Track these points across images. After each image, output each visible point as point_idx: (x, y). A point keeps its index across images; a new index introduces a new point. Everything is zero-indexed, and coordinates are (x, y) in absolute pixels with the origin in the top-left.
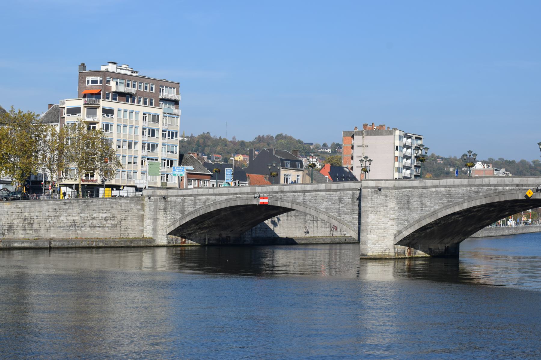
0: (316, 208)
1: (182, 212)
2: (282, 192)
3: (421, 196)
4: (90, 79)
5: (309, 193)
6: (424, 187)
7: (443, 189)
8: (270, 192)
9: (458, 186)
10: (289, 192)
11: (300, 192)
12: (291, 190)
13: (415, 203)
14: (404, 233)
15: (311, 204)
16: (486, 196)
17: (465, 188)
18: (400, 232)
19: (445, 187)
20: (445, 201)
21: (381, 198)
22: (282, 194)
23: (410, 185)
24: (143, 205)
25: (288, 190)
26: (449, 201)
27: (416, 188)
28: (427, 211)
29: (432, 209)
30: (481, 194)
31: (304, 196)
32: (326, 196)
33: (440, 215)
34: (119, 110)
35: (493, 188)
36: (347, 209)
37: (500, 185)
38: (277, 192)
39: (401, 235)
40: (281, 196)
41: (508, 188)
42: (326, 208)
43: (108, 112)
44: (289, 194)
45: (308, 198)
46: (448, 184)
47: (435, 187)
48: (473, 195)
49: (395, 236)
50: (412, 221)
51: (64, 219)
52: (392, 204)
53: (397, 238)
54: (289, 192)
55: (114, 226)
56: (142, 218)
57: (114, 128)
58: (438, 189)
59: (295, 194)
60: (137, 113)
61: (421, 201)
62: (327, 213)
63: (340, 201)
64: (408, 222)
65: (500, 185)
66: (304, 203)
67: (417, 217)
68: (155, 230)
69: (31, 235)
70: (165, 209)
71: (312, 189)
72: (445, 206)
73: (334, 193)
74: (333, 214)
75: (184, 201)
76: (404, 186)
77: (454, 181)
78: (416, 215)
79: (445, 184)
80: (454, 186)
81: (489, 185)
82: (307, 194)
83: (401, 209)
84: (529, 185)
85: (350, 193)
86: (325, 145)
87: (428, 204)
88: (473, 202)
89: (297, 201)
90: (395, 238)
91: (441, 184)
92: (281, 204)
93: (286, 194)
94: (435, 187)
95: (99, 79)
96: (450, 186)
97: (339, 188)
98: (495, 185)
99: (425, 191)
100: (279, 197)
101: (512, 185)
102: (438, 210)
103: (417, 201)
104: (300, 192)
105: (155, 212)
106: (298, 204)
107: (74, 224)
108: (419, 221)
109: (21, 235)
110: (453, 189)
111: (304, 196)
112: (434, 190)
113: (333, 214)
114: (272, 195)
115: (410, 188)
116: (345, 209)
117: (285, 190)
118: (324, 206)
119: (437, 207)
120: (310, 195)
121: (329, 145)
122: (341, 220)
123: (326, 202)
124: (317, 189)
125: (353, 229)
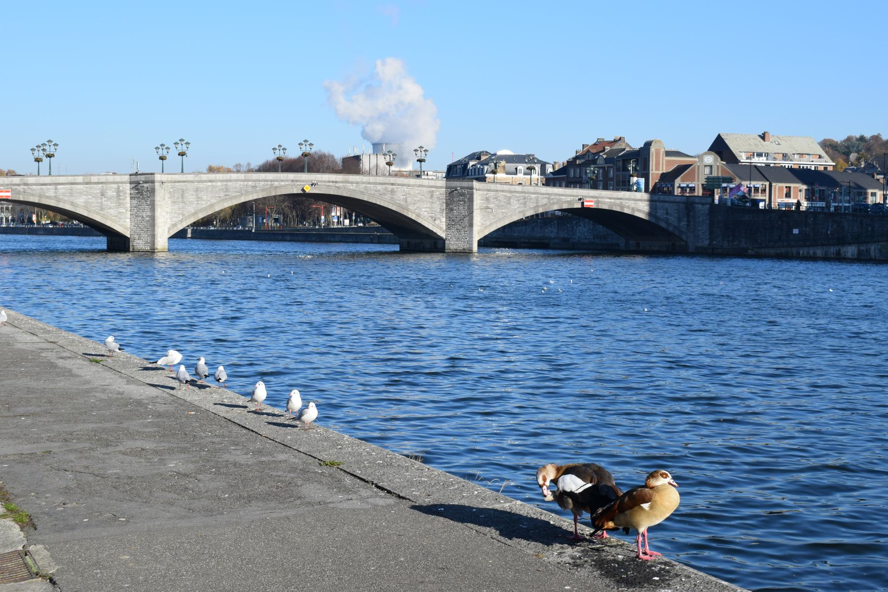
0: (72, 202)
2: (25, 184)
3: (197, 190)
5: (62, 186)
6: (199, 182)
7: (219, 184)
8: (8, 185)
9: (235, 181)
10: (35, 184)
11: (50, 184)
12: (37, 182)
13: (190, 197)
14: (179, 226)
15: (66, 198)
16: (263, 190)
17: (242, 183)
18: (174, 225)
19: (222, 181)
20: (222, 194)
22: (25, 187)
23: (184, 180)
25: (34, 182)
26: (226, 195)
27: (192, 182)
28: (204, 204)
29: (209, 202)
30: (258, 189)
31: (56, 189)
32: (85, 189)
35: (269, 183)
36: (111, 203)
37: (277, 181)
38: (19, 185)
39: (175, 228)
40: (24, 189)
41: (283, 183)
42: (86, 203)
44: (35, 187)
45: (60, 191)
46: (225, 178)
47: (211, 181)
48: (250, 189)
49: (169, 229)
50: (187, 214)
53: (171, 231)
54: (35, 184)
58: (214, 184)
59: (44, 187)
61: (198, 195)
62: (87, 207)
64: (183, 215)
65: (277, 181)
66: (56, 197)
67: (193, 211)
71: (66, 182)
72: (223, 200)
73: (95, 186)
74: (94, 208)
76: (178, 180)
77: (231, 176)
79: (221, 178)
80: (230, 181)
81: (267, 181)
82: (59, 187)
83: (174, 202)
84: (306, 181)
85: (115, 186)
87: (205, 198)
88: (250, 196)
89: (47, 195)
90: (169, 231)
91: (217, 179)
92: (24, 198)
93: (31, 187)
94: (211, 181)
96: (227, 181)
97: (100, 181)
98: (272, 181)
99: (201, 185)
100: (22, 190)
101: (287, 181)
102: (215, 203)
103: (192, 195)
104: (50, 184)
106: (49, 198)
108: (196, 213)
110: (230, 183)
111: (56, 189)
112: (210, 184)
113: (94, 208)
114: (11, 188)
115: (184, 182)
116: (109, 203)
117: (29, 182)
118: (83, 200)
119: (213, 201)
120: (63, 188)
122: (104, 214)
123: (85, 195)
124: (73, 181)
125: (120, 224)
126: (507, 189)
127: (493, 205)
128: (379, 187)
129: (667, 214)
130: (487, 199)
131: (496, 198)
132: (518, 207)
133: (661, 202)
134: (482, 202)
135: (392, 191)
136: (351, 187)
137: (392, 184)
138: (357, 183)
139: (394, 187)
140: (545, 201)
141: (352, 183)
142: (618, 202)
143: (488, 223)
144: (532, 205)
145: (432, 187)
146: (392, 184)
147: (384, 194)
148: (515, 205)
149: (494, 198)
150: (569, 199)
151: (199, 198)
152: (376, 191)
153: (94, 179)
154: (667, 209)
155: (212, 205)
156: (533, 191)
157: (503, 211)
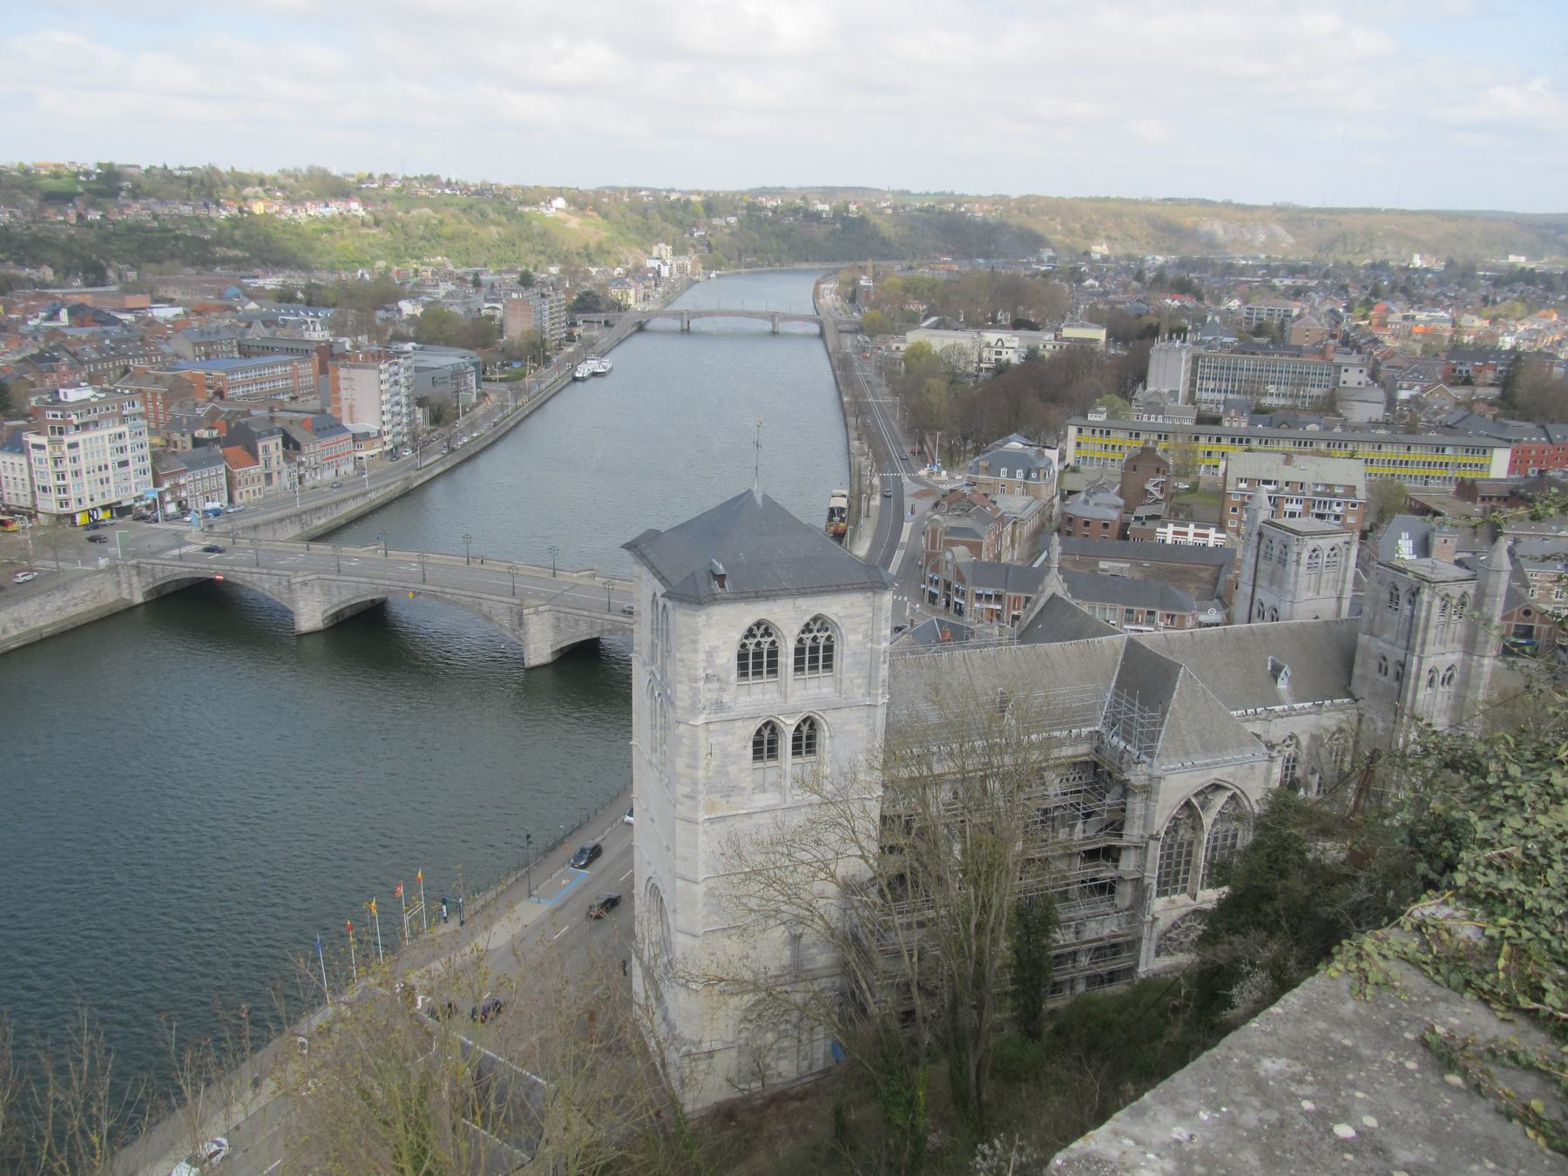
1: (153, 576)
3: (338, 587)
4: (50, 413)
21: (307, 589)
24: (118, 574)
28: (343, 598)
34: (85, 440)
43: (73, 446)
51: (48, 608)
52: (317, 590)
55: (94, 598)
56: (118, 584)
57: (82, 457)
60: (102, 437)
63: (280, 583)
68: (131, 594)
69: (23, 629)
70: (139, 574)
75: (153, 570)
78: (335, 601)
86: (370, 176)
95: (59, 413)
105: (129, 578)
107: (59, 609)
109: (15, 633)
121: (376, 176)
130: (558, 619)
131: (566, 619)
135: (480, 604)
140: (610, 627)
144: (599, 629)
148: (583, 627)
151: (340, 593)
153: (274, 572)
155: (349, 600)
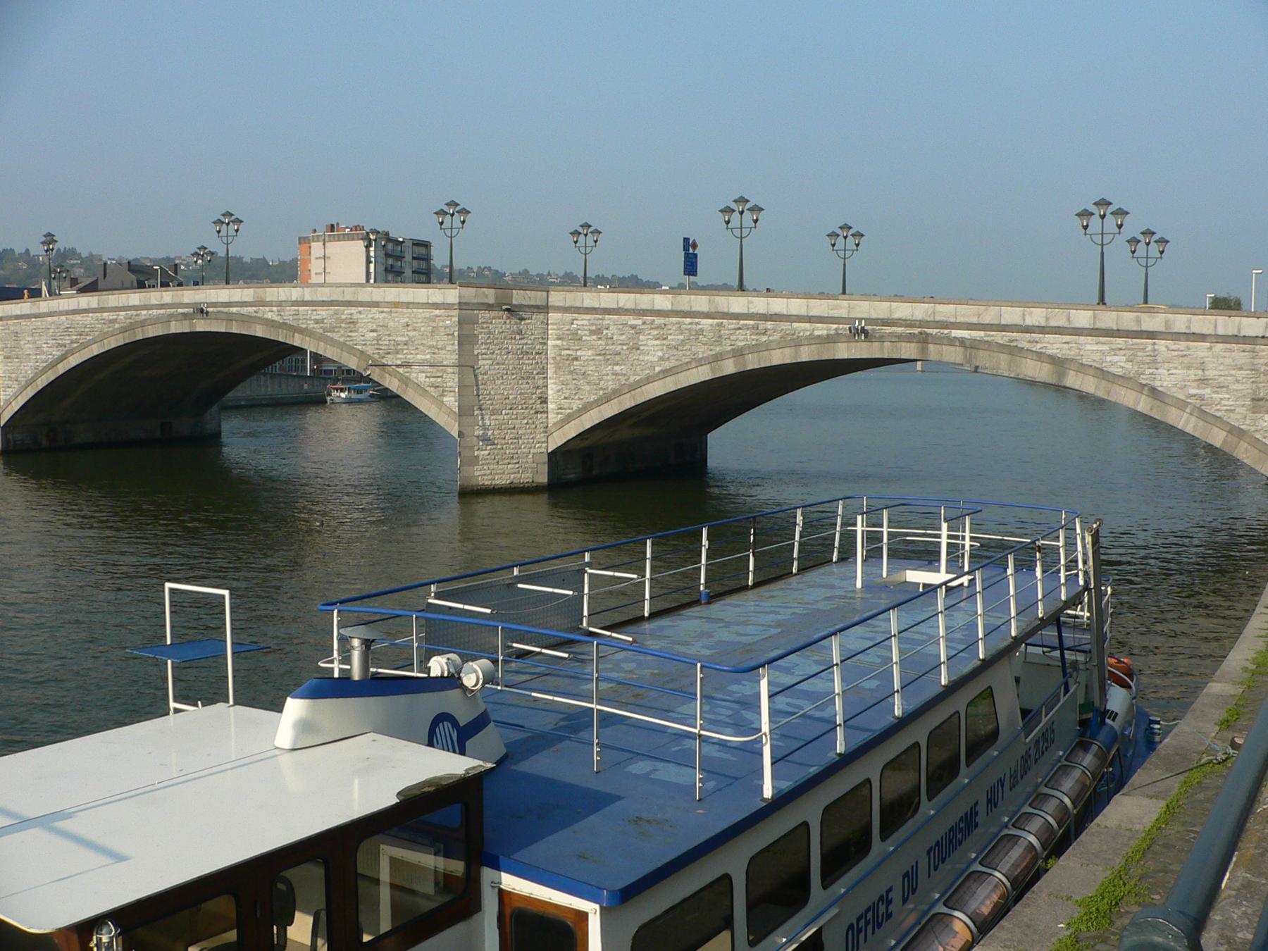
16: (124, 330)
33: (62, 368)
126: (630, 305)
127: (590, 353)
128: (322, 312)
129: (1203, 381)
131: (597, 332)
132: (661, 359)
133: (1177, 336)
134: (559, 343)
136: (269, 316)
137: (349, 304)
138: (280, 304)
139: (353, 310)
140: (743, 338)
141: (270, 304)
142: (1000, 337)
143: (576, 405)
145: (436, 306)
146: (349, 304)
147: (332, 330)
149: (592, 333)
150: (821, 330)
152: (317, 322)
154: (1202, 366)
155: (54, 365)
156: (705, 309)
157: (617, 368)
